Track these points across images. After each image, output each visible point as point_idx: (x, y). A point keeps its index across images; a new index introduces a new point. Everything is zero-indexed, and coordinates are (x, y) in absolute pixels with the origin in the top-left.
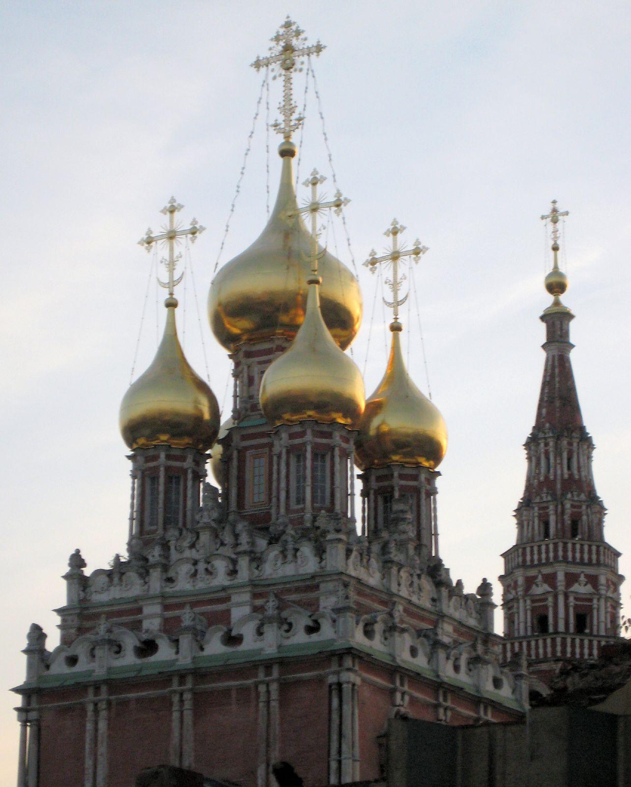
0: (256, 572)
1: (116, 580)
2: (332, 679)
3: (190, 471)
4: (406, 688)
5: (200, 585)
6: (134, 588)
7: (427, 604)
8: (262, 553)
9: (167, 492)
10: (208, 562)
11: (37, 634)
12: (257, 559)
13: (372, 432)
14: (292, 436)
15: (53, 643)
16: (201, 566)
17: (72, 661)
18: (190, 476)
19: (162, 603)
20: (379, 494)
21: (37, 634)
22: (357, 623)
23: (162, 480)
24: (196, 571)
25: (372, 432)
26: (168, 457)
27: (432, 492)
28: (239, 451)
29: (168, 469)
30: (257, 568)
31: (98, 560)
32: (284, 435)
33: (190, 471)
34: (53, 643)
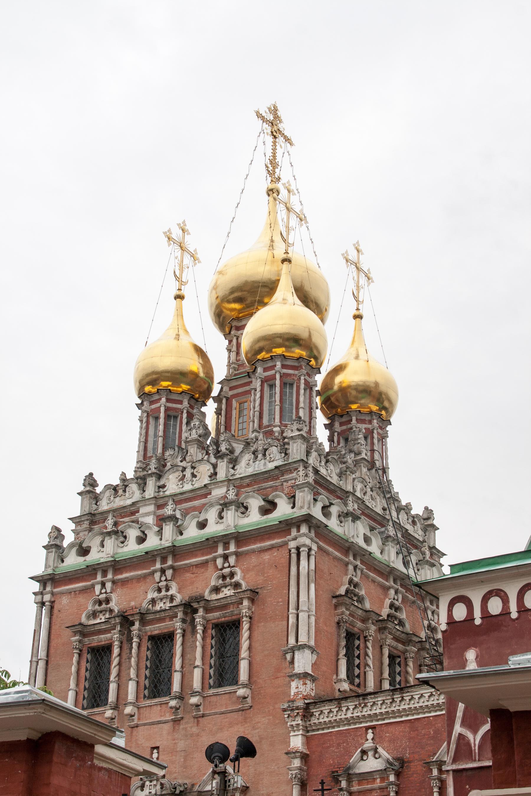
0: (232, 471)
1: (120, 492)
2: (292, 545)
3: (185, 411)
4: (358, 563)
5: (188, 487)
6: (134, 493)
7: (379, 510)
8: (237, 457)
9: (165, 425)
10: (193, 468)
11: (57, 533)
12: (234, 462)
13: (336, 388)
14: (265, 370)
15: (69, 538)
16: (188, 473)
17: (84, 552)
18: (185, 415)
19: (155, 504)
20: (341, 434)
21: (57, 533)
22: (315, 500)
23: (162, 421)
24: (184, 476)
25: (336, 388)
26: (168, 400)
27: (383, 438)
28: (228, 399)
29: (167, 409)
30: (233, 468)
31: (107, 478)
32: (260, 370)
33: (185, 411)
34: (69, 538)
